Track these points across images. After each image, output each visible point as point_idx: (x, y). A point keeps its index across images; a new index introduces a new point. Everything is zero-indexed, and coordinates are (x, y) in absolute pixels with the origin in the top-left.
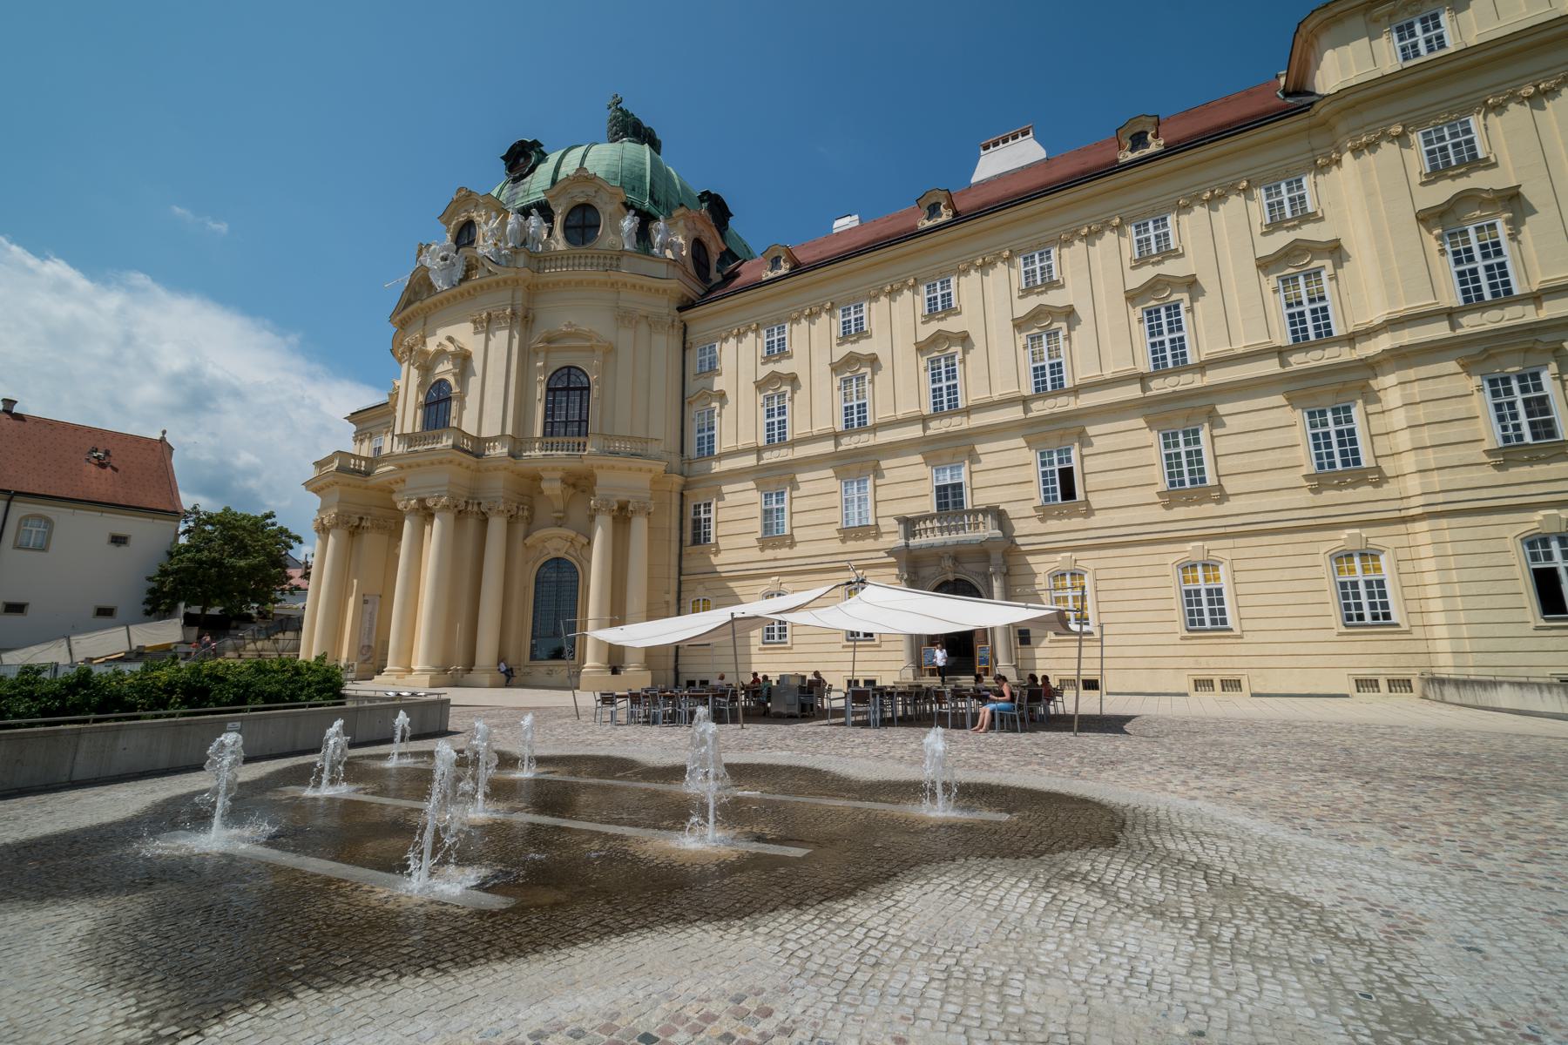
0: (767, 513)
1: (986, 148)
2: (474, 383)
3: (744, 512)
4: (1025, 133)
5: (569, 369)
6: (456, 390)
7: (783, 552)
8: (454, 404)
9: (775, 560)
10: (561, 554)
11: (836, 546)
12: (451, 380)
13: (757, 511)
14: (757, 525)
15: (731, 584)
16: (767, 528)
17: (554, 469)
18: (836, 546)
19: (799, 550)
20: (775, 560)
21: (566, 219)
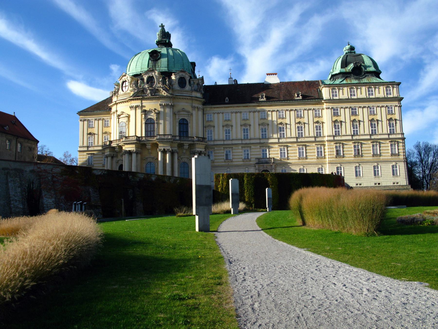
0: (227, 155)
1: (268, 74)
4: (276, 74)
5: (184, 119)
8: (156, 125)
10: (185, 161)
11: (242, 163)
14: (225, 157)
16: (227, 159)
21: (178, 81)
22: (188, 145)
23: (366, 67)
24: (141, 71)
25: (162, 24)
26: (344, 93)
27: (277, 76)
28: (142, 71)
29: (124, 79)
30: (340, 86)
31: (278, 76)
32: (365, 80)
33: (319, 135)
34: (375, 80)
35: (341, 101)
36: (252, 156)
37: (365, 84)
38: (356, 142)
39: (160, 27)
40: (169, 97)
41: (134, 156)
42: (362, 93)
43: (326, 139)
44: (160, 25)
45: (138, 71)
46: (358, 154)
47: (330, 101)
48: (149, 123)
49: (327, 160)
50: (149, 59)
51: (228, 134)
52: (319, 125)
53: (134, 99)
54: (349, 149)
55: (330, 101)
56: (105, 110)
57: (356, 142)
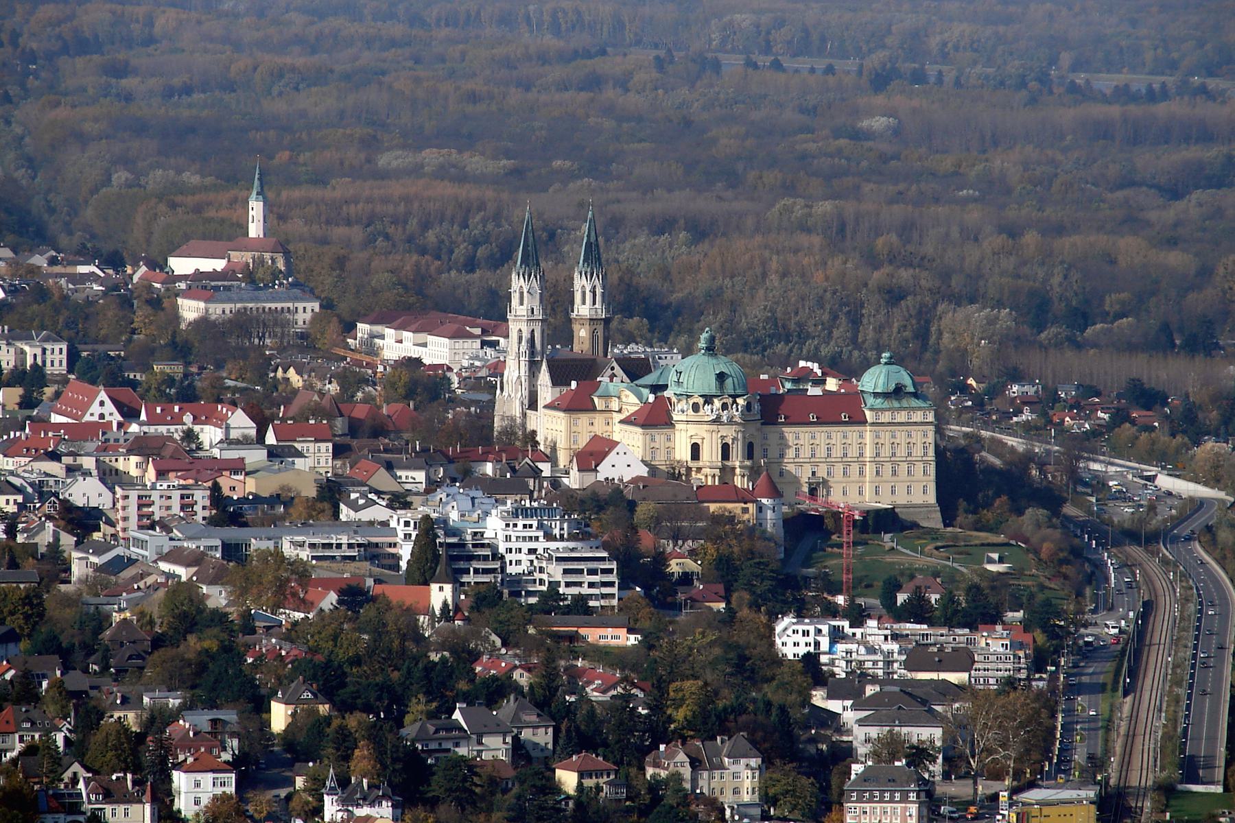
23: (906, 387)
26: (886, 417)
29: (695, 400)
30: (882, 410)
32: (905, 403)
33: (861, 455)
34: (915, 403)
35: (882, 424)
37: (905, 409)
38: (893, 462)
41: (717, 478)
42: (902, 417)
43: (868, 459)
45: (706, 392)
46: (894, 473)
47: (873, 424)
49: (868, 478)
52: (861, 446)
54: (888, 468)
55: (873, 424)
56: (666, 424)
57: (893, 462)
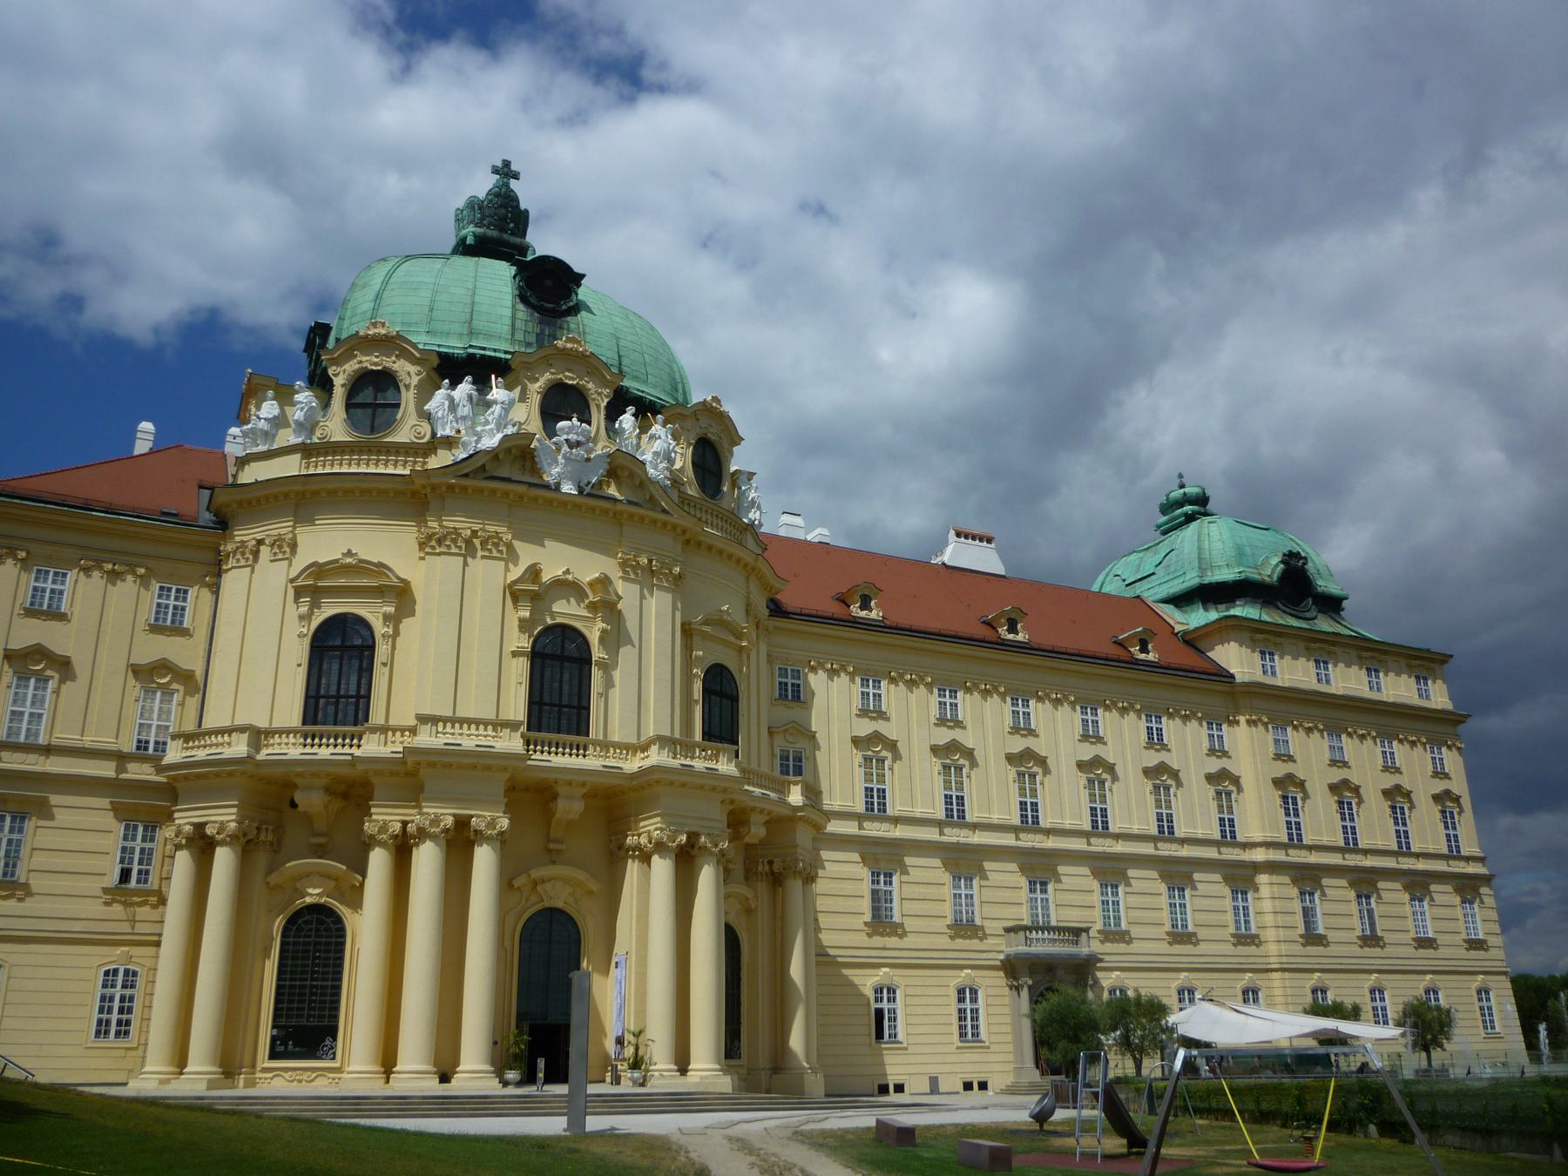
2: (626, 654)
3: (848, 888)
4: (989, 541)
6: (597, 653)
7: (892, 941)
8: (596, 675)
9: (884, 949)
11: (944, 942)
12: (594, 637)
13: (866, 887)
14: (866, 905)
15: (846, 972)
16: (876, 910)
17: (762, 811)
18: (944, 942)
19: (909, 941)
20: (884, 949)
22: (767, 823)
24: (471, 346)
25: (507, 164)
27: (993, 545)
28: (484, 349)
31: (997, 549)
36: (989, 911)
39: (495, 171)
40: (675, 527)
44: (499, 164)
48: (553, 657)
50: (514, 296)
51: (875, 786)
53: (464, 489)
